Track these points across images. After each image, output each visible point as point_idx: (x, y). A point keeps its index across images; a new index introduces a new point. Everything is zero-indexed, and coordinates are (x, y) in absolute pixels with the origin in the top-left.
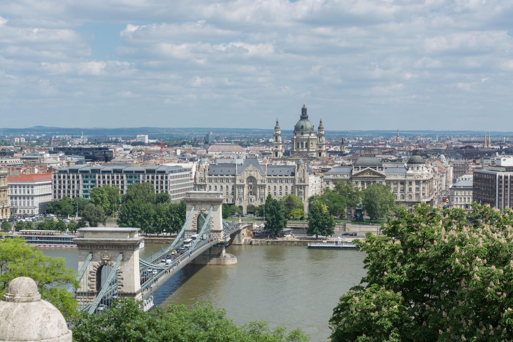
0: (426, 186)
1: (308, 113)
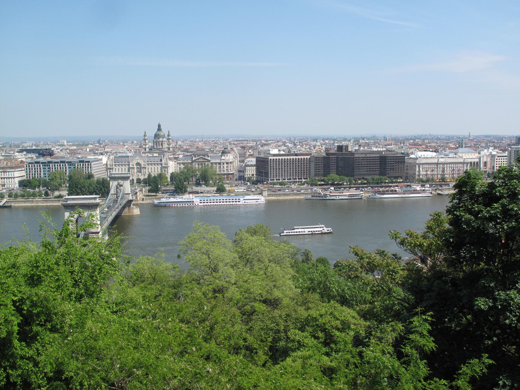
0: (232, 165)
1: (161, 127)
